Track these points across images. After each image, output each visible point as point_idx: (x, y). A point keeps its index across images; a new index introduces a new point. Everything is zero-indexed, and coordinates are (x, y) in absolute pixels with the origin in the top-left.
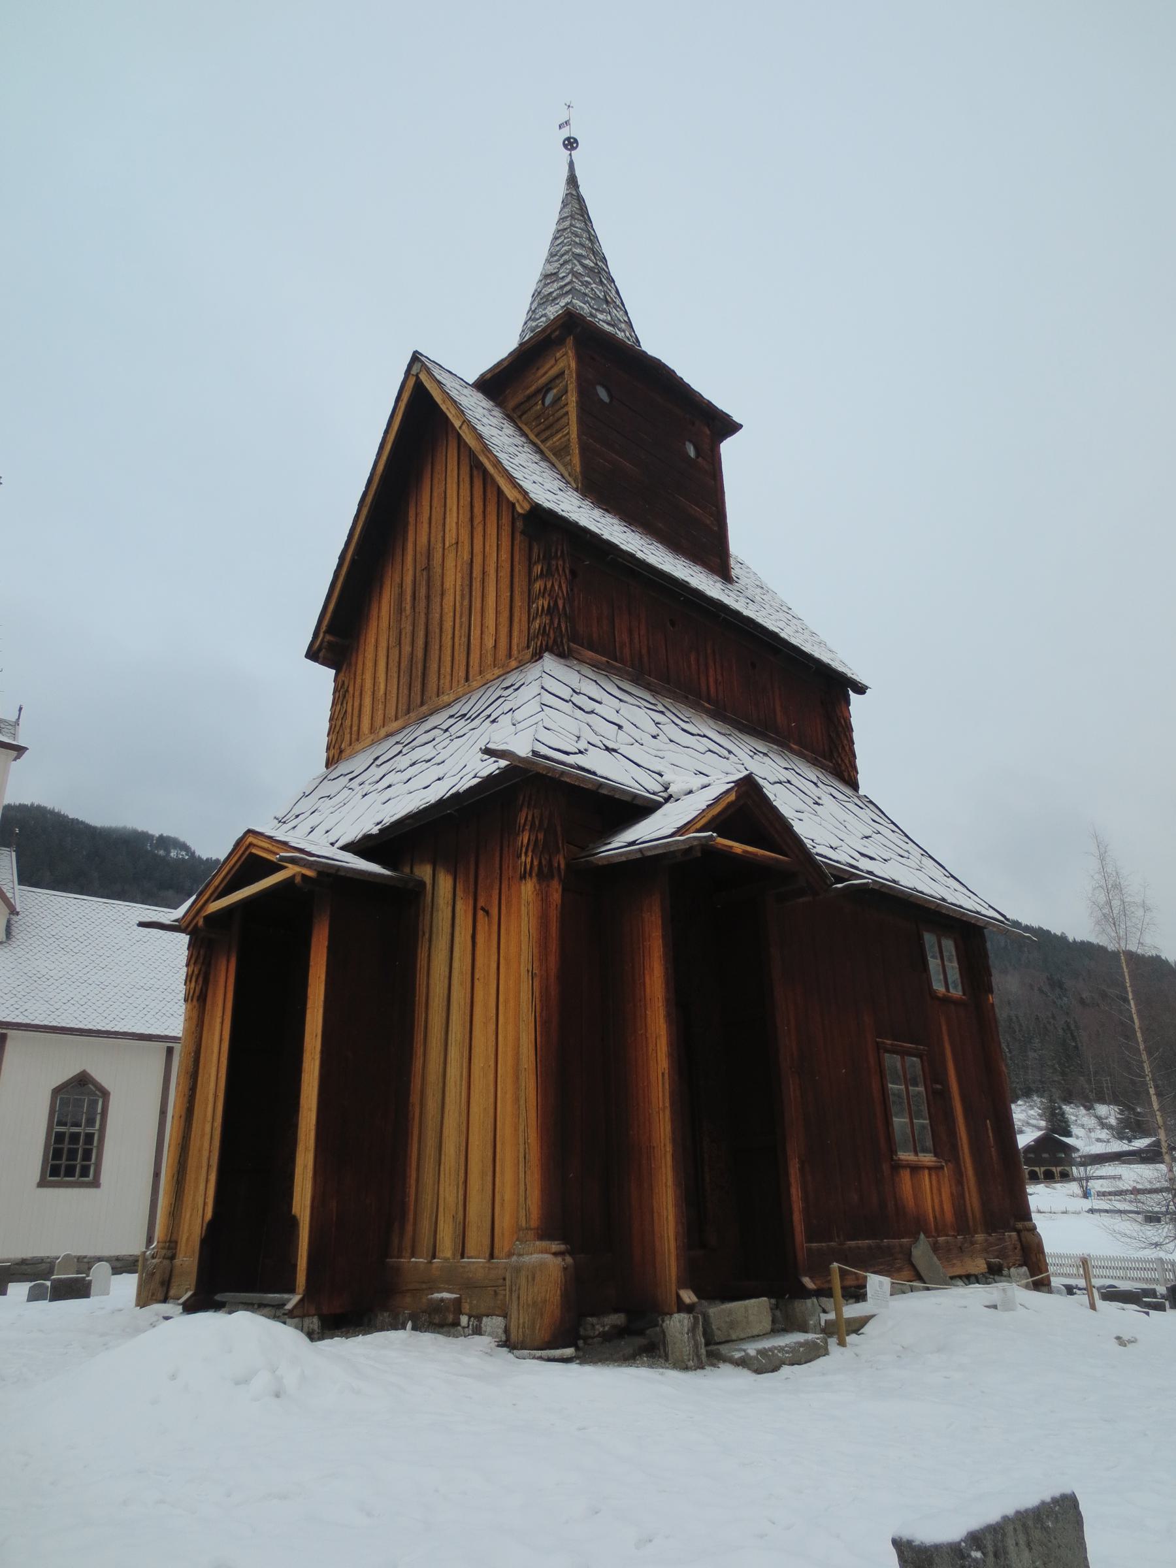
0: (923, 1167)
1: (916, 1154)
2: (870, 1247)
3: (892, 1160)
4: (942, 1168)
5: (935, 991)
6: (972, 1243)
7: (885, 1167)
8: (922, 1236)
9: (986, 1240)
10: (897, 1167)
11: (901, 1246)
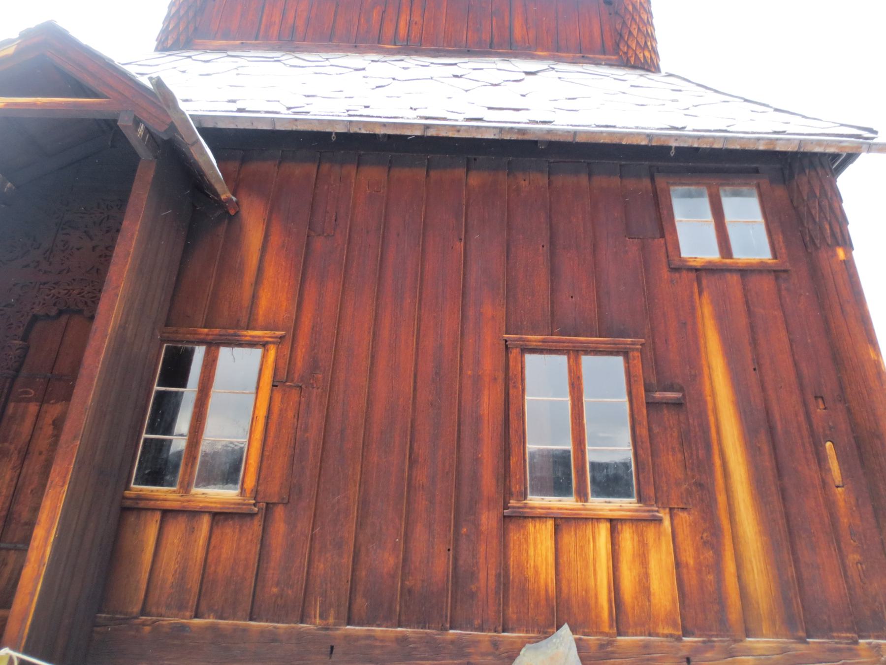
0: (598, 520)
1: (582, 496)
2: (403, 640)
3: (506, 507)
4: (660, 520)
5: (685, 260)
6: (731, 654)
7: (488, 520)
8: (565, 629)
9: (784, 651)
10: (523, 517)
11: (495, 644)
